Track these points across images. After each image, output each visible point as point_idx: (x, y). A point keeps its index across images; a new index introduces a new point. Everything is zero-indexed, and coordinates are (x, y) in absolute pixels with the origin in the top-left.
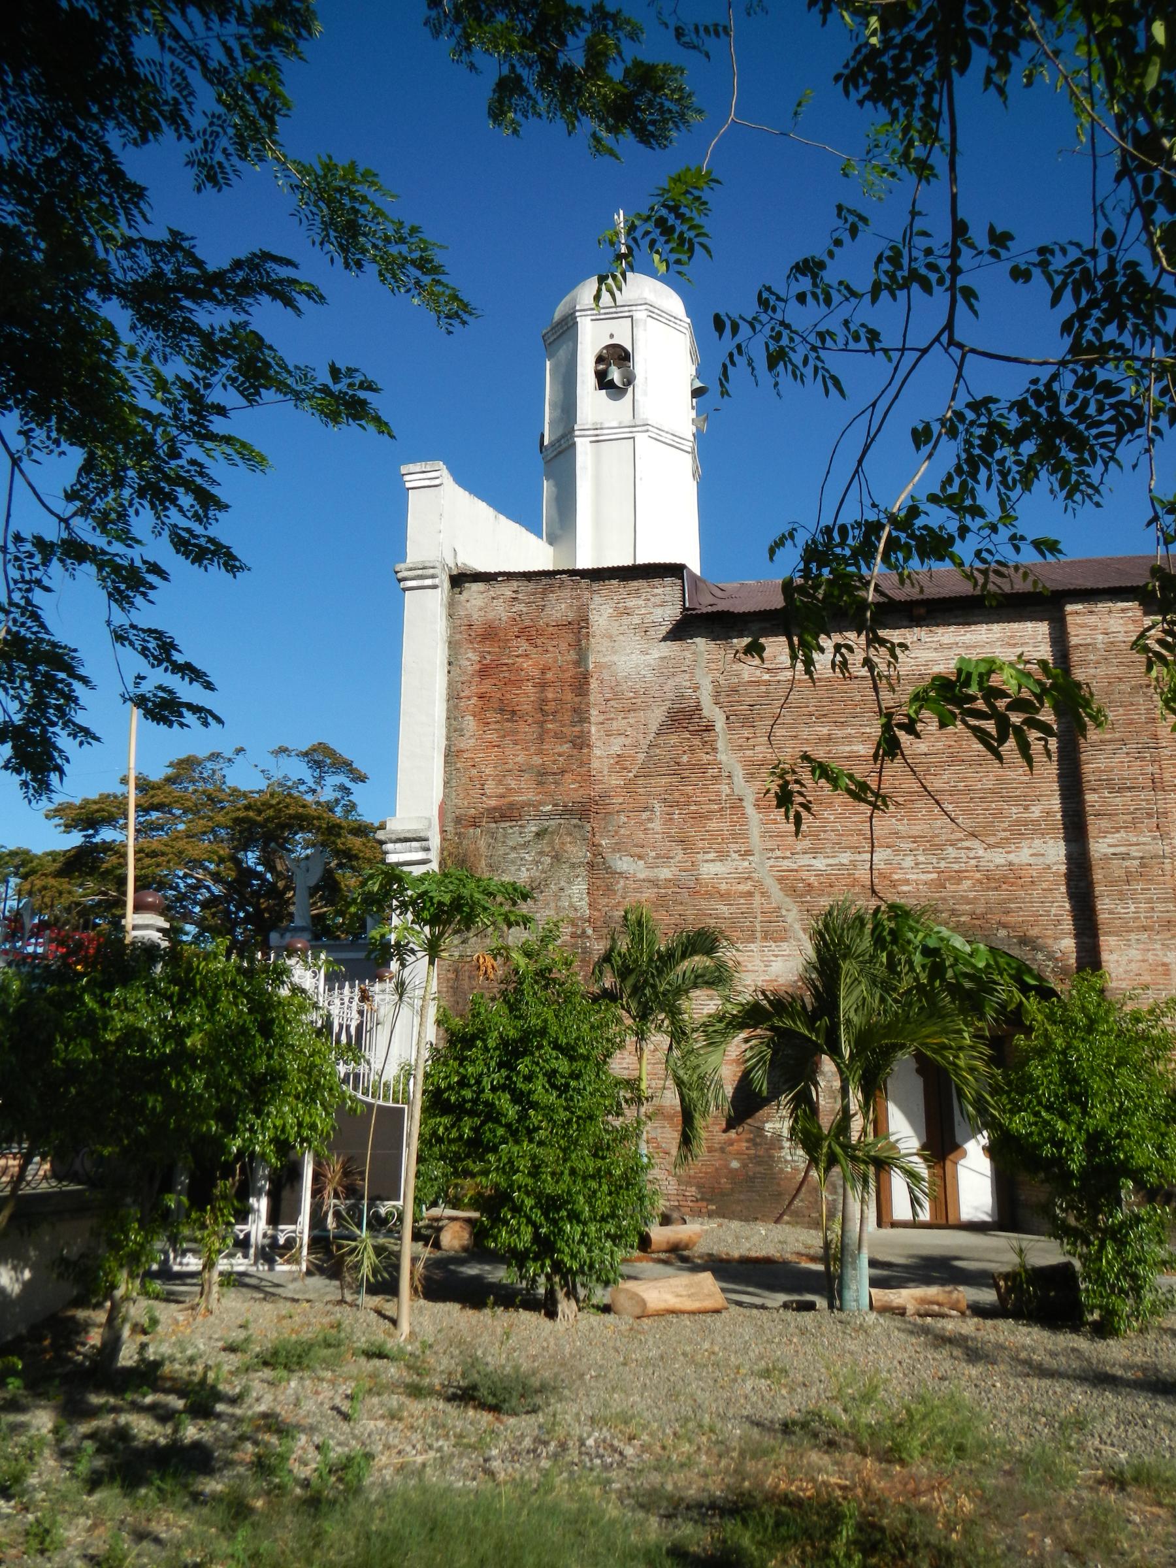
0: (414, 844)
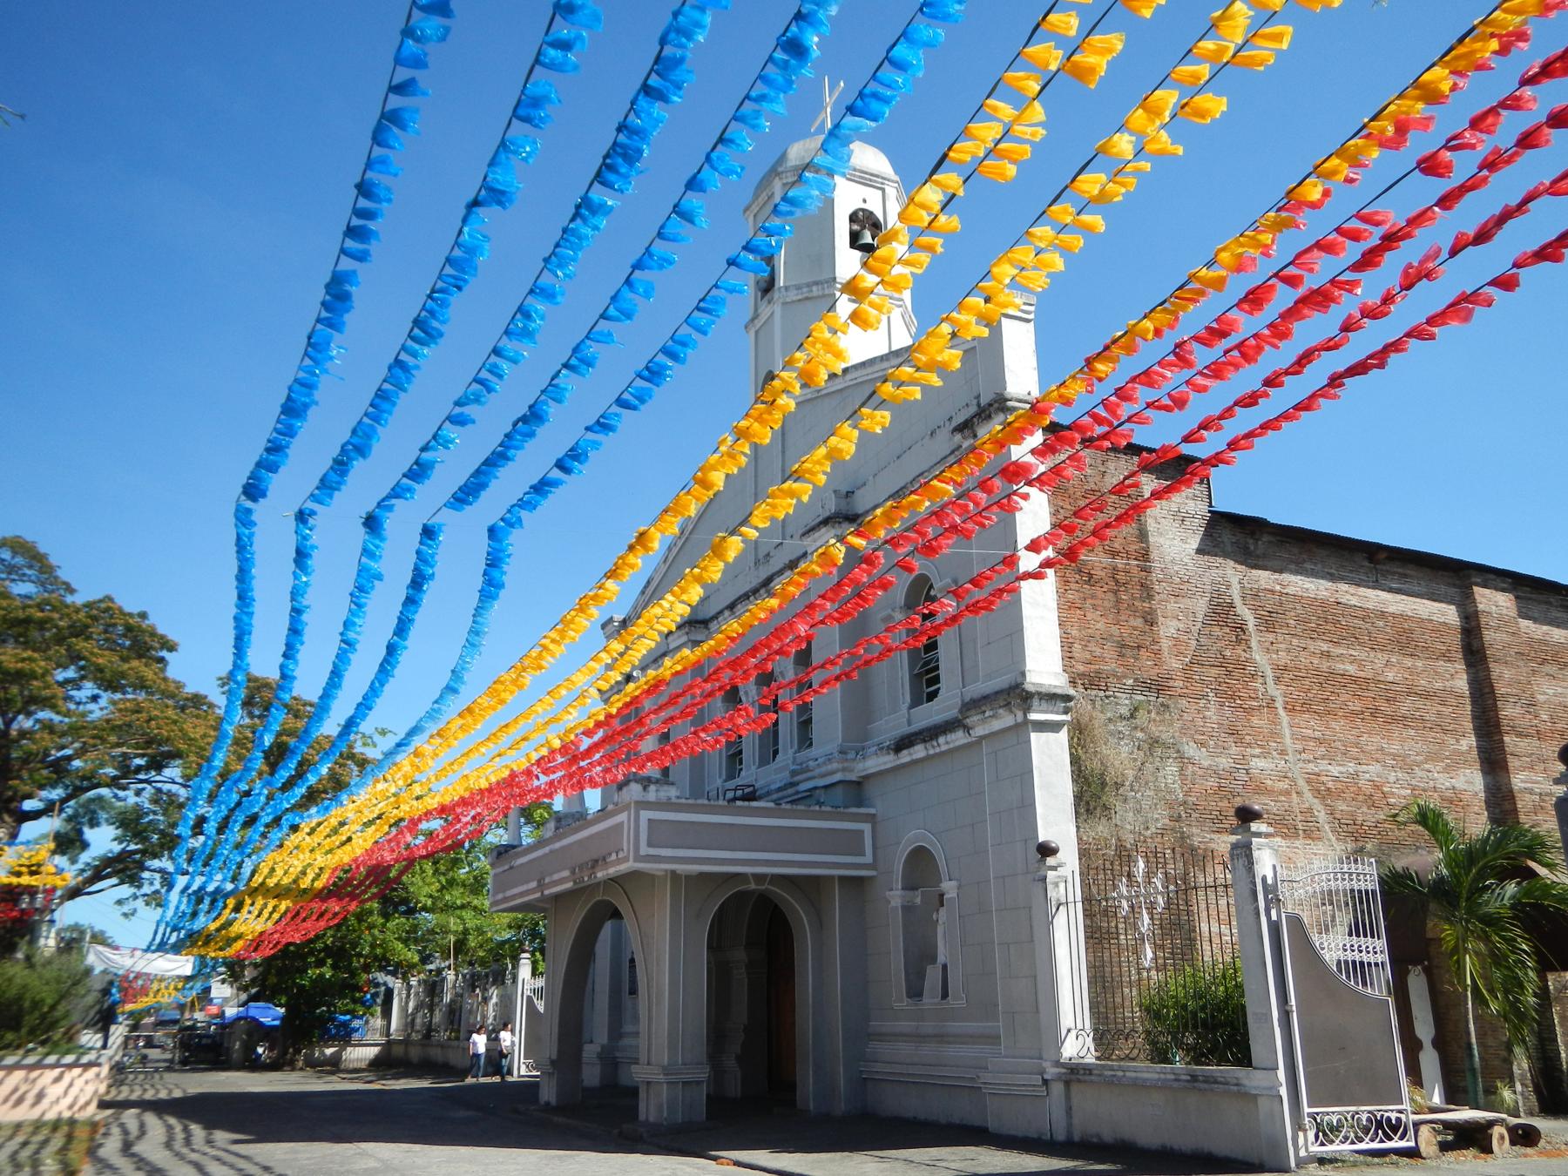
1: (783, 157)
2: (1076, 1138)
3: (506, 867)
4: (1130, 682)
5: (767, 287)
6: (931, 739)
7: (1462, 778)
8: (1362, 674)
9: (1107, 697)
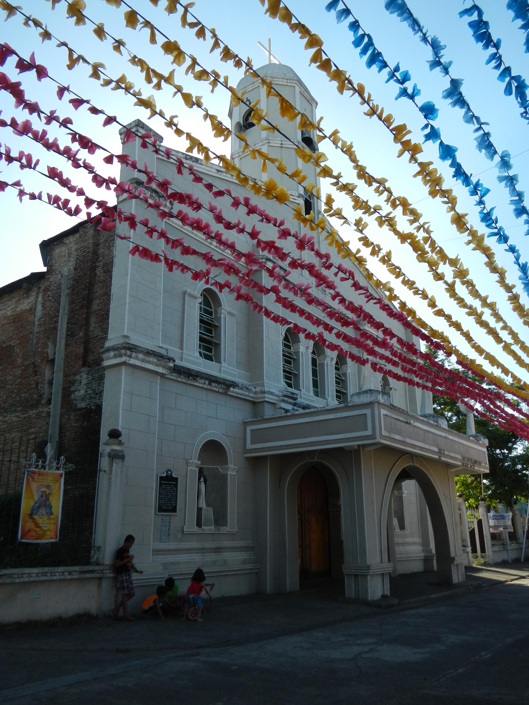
3: (402, 419)
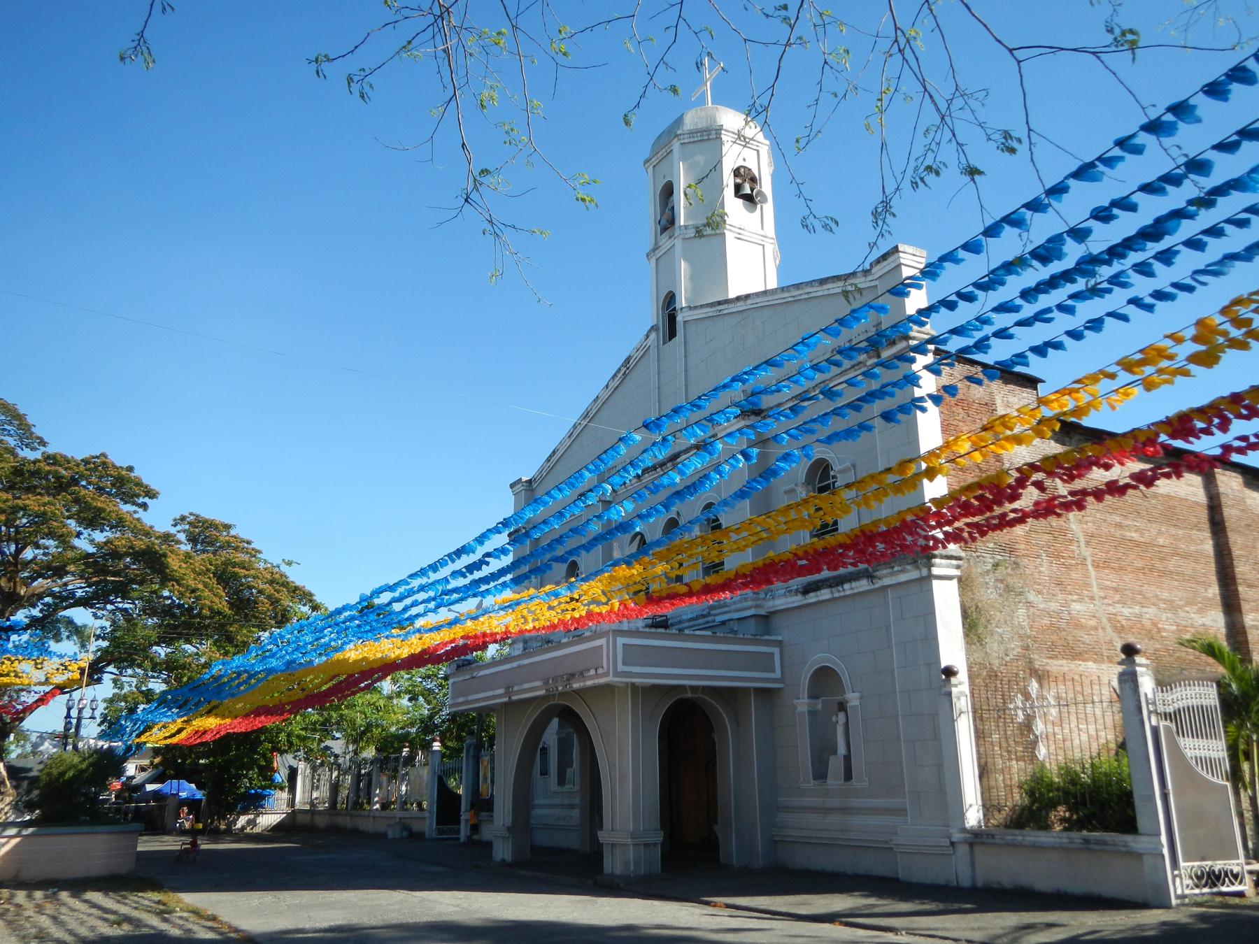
0: (954, 562)
1: (679, 121)
2: (979, 884)
3: (467, 677)
4: (991, 545)
5: (667, 222)
6: (837, 585)
7: (1210, 618)
8: (1142, 540)
9: (978, 557)
